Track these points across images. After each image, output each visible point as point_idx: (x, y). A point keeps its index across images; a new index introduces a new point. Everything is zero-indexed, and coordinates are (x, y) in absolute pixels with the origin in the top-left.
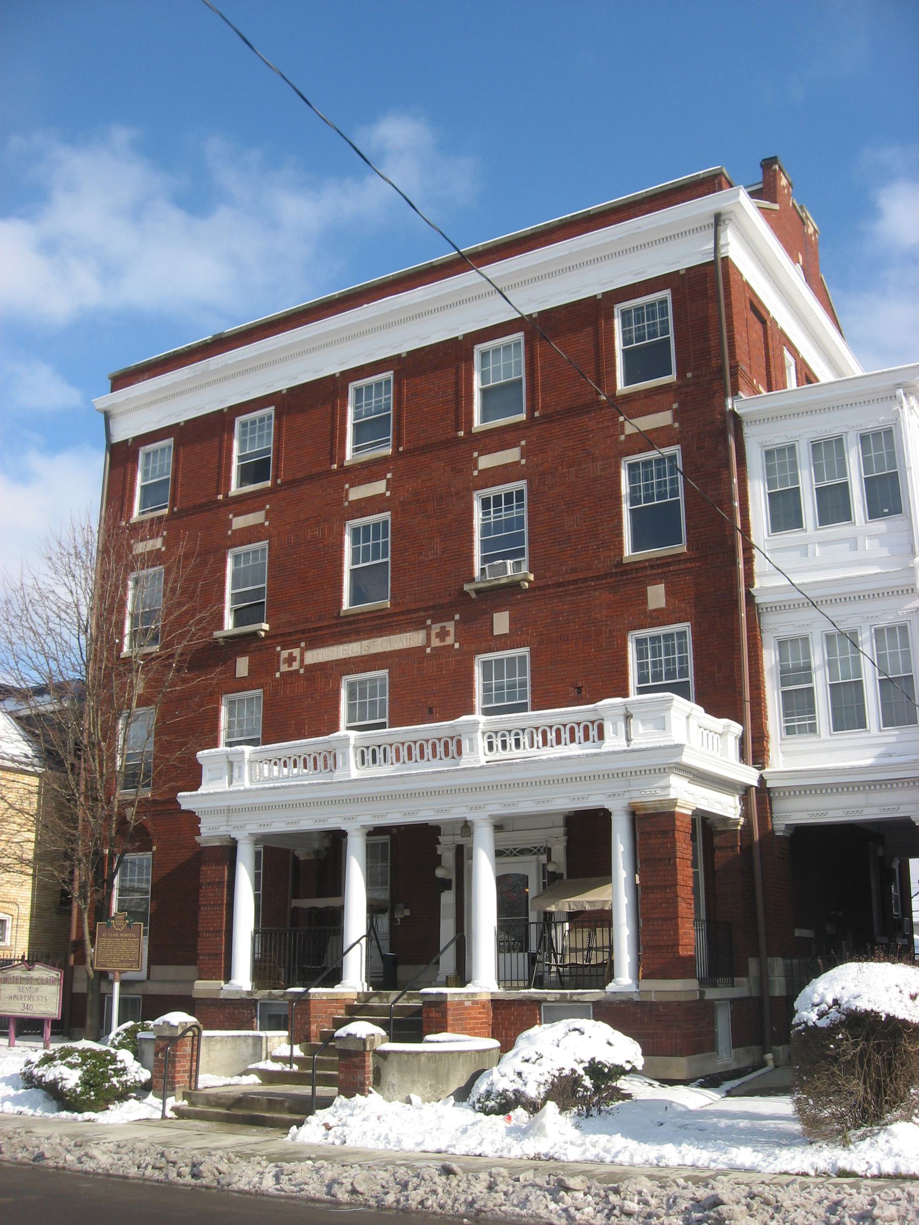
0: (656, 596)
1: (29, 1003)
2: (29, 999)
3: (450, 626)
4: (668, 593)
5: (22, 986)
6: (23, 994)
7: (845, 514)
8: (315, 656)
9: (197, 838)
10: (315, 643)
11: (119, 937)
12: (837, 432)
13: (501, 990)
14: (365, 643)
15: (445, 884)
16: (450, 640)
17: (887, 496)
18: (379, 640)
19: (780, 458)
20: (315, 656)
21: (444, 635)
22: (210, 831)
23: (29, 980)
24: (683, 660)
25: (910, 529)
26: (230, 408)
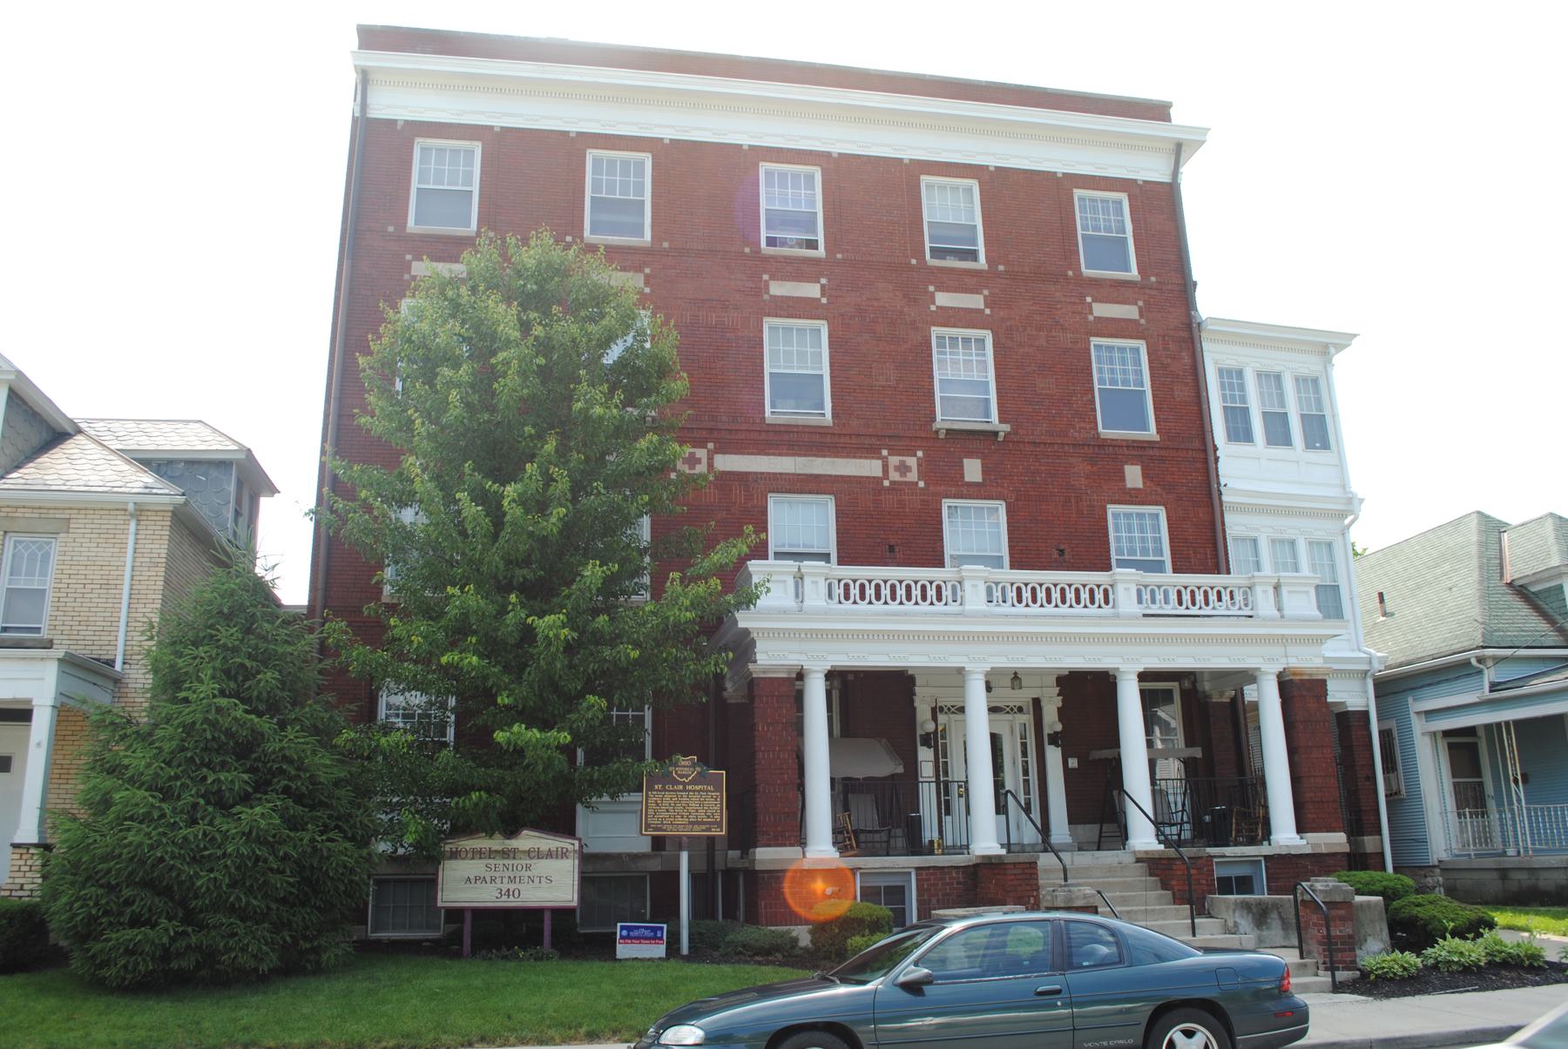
0: (1133, 476)
1: (512, 887)
2: (512, 880)
3: (912, 462)
4: (1145, 476)
5: (492, 862)
6: (493, 874)
7: (1287, 441)
8: (729, 463)
9: (751, 666)
10: (724, 448)
11: (685, 790)
12: (1277, 369)
13: (1162, 847)
14: (799, 459)
15: (1054, 739)
16: (913, 476)
17: (1319, 433)
18: (820, 460)
19: (1232, 378)
20: (729, 463)
21: (908, 468)
22: (770, 657)
23: (505, 854)
24: (1158, 541)
25: (1341, 466)
26: (580, 134)
